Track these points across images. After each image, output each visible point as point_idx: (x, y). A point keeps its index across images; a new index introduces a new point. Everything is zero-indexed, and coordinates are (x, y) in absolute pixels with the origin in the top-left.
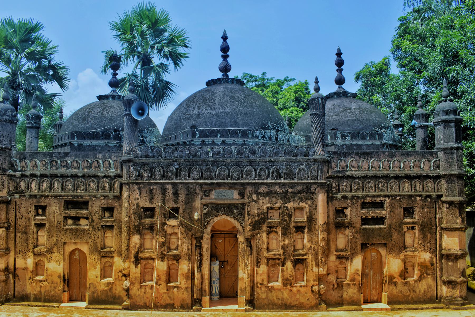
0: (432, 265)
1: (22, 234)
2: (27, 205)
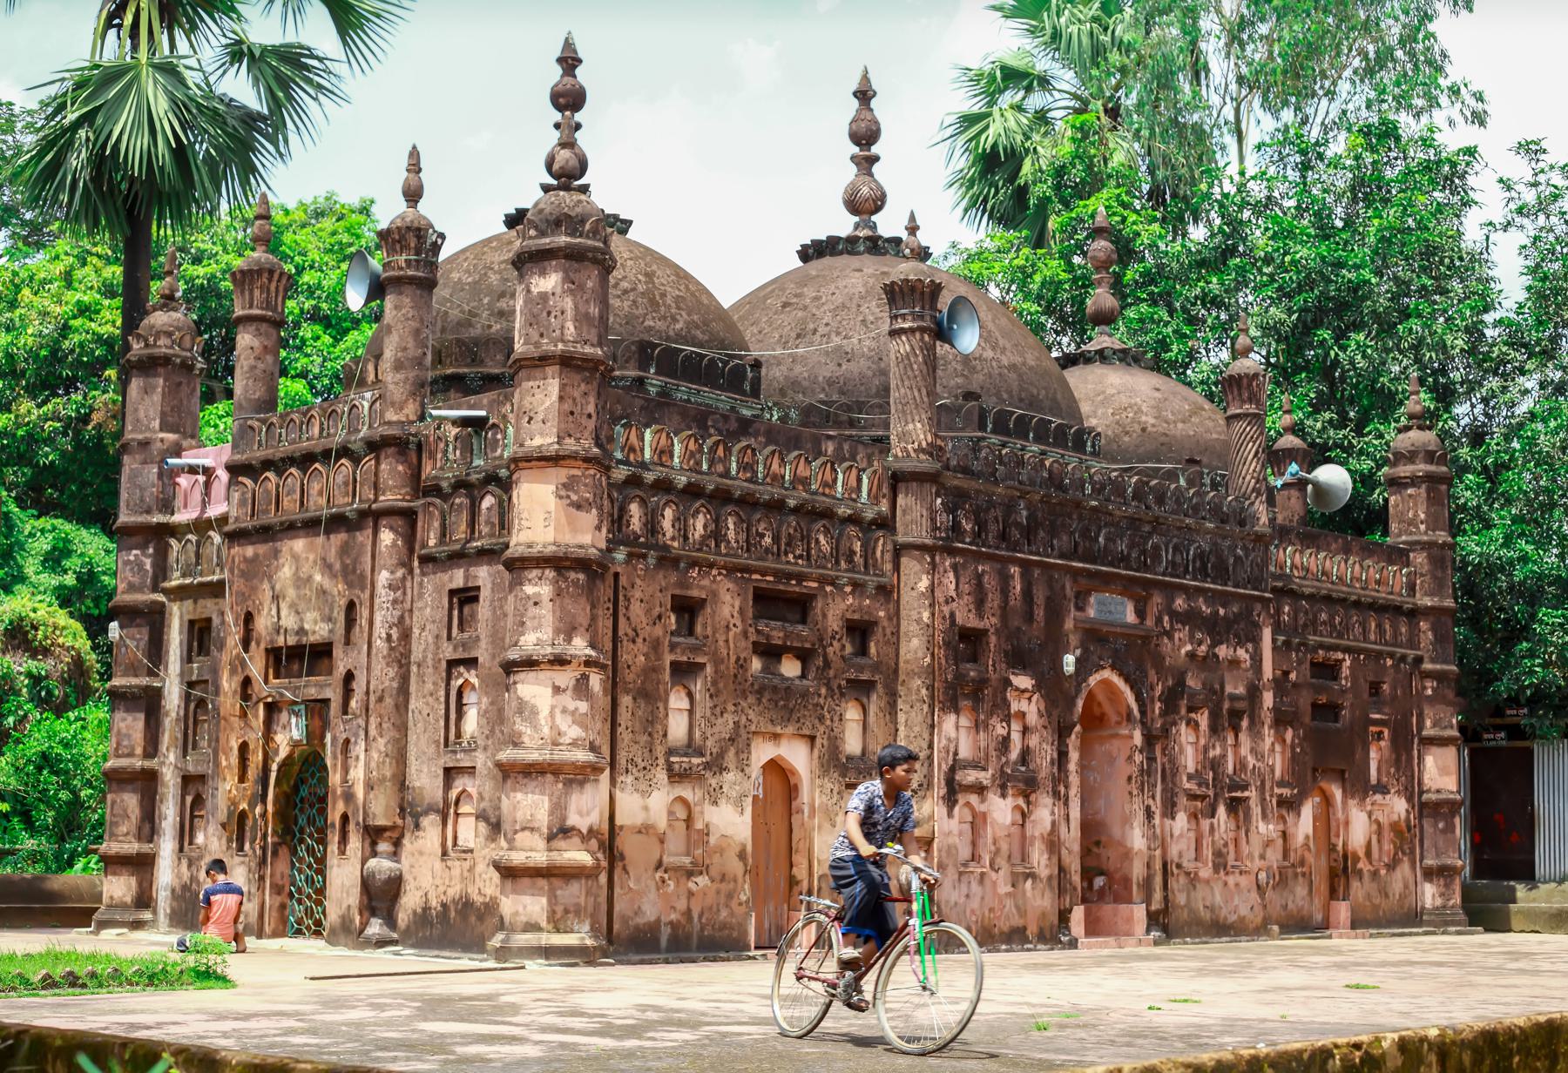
0: (1409, 829)
2: (650, 590)
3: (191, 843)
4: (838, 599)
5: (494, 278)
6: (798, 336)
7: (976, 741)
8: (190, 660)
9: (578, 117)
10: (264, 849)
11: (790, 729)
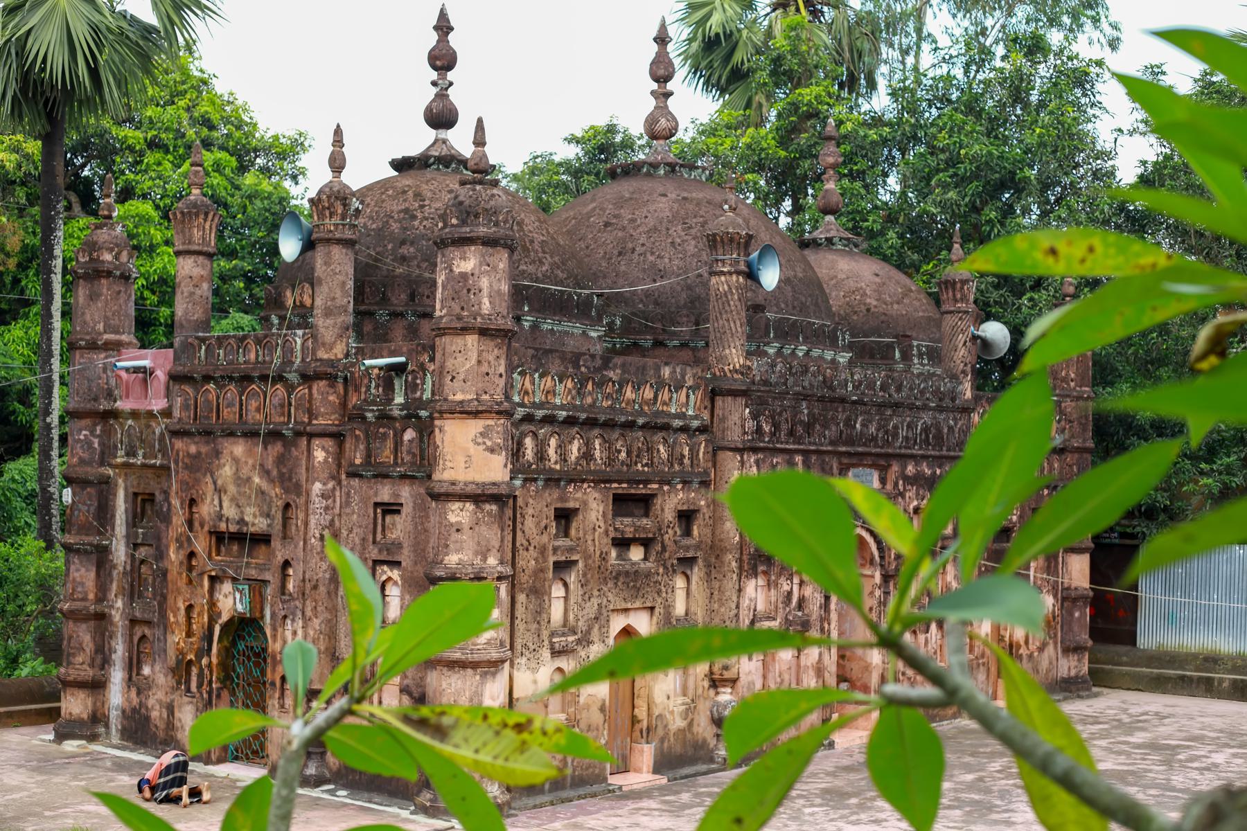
0: (1054, 617)
1: (527, 596)
2: (539, 506)
3: (138, 674)
4: (672, 495)
5: (395, 226)
6: (620, 254)
7: (768, 597)
8: (134, 526)
9: (451, 75)
10: (210, 693)
11: (638, 604)
